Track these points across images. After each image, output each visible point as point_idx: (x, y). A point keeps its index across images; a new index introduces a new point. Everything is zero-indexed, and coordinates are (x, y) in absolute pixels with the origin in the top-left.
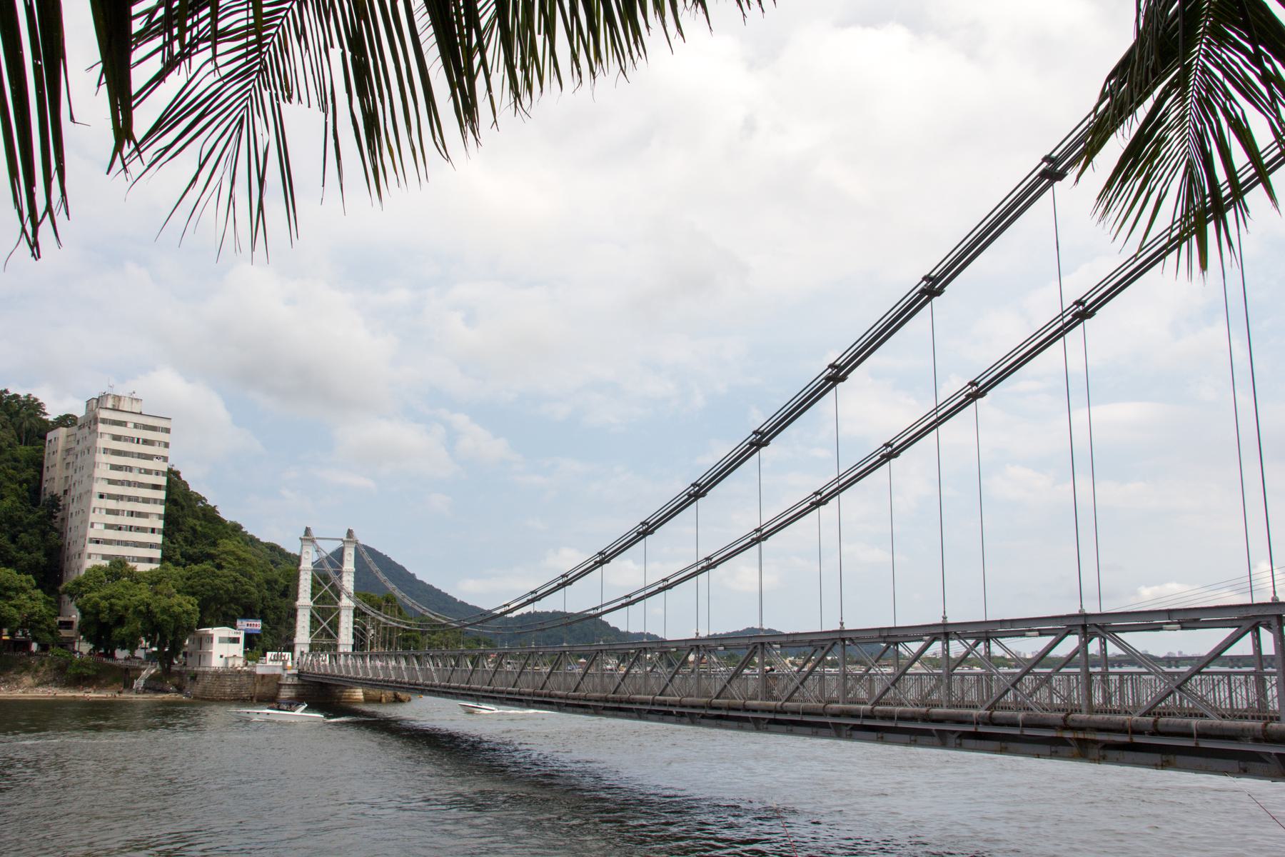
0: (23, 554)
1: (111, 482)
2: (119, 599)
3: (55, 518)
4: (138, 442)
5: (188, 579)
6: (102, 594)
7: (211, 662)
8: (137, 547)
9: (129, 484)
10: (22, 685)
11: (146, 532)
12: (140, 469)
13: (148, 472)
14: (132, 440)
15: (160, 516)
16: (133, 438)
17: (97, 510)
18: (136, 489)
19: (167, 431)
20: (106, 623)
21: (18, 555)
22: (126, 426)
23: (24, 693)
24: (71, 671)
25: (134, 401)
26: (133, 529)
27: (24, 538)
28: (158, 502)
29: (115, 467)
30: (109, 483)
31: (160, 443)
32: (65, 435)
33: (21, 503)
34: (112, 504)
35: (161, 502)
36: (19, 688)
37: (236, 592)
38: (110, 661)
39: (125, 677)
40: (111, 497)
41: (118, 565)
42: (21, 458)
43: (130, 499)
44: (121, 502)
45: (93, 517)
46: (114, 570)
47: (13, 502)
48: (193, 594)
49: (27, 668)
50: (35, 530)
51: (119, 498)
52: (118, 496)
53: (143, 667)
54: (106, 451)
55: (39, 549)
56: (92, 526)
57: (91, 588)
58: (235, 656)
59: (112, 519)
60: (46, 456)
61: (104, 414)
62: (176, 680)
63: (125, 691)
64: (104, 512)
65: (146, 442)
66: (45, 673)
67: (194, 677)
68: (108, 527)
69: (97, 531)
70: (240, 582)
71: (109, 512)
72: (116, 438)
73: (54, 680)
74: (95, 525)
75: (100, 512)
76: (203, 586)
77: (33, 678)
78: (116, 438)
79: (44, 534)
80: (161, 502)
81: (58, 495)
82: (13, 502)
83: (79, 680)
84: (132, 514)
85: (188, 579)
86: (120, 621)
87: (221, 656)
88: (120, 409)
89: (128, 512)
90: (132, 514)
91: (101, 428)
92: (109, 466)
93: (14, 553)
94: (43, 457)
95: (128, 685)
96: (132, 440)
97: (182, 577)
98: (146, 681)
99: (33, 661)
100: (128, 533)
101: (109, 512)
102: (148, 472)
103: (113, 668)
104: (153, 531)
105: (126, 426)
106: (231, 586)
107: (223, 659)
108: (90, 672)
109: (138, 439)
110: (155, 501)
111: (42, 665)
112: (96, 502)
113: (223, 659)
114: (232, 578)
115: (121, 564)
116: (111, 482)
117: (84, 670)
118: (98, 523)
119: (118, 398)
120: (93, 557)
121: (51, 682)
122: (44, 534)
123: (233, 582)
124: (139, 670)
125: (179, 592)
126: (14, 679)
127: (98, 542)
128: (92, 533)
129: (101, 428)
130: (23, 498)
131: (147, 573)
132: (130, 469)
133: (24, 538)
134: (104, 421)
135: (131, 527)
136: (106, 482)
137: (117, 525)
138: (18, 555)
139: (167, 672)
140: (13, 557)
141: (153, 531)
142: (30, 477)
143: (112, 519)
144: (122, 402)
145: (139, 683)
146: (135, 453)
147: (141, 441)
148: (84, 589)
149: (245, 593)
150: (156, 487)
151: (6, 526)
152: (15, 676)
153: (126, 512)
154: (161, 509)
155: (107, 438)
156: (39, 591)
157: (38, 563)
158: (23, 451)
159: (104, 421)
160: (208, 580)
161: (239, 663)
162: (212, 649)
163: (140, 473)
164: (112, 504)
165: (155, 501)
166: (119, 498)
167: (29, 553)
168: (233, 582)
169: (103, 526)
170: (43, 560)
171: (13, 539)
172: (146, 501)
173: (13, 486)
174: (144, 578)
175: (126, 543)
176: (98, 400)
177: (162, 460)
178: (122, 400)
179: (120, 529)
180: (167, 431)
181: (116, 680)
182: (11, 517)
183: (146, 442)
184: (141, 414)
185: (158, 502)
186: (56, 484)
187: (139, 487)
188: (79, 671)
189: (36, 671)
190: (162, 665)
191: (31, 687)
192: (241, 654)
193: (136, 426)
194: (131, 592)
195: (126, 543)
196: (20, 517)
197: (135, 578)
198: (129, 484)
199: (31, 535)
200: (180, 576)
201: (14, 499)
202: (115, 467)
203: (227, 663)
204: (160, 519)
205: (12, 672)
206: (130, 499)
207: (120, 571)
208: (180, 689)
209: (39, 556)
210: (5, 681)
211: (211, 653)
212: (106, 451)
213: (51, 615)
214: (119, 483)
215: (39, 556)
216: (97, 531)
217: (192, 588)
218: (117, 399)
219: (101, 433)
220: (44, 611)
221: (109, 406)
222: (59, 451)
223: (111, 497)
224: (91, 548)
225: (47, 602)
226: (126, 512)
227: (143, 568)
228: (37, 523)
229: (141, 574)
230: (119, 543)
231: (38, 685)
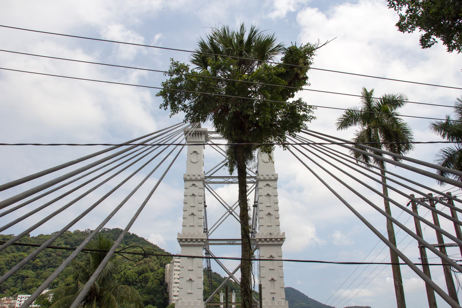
3: (167, 289)
17: (175, 287)
27: (158, 295)
45: (174, 289)
50: (161, 293)
54: (176, 270)
56: (174, 291)
64: (177, 287)
79: (163, 294)
82: (155, 285)
112: (175, 285)
120: (175, 301)
127: (175, 296)
128: (174, 294)
133: (158, 295)
140: (155, 301)
196: (157, 290)
209: (161, 301)
212: (176, 270)
215: (161, 301)
224: (174, 298)
228: (161, 291)
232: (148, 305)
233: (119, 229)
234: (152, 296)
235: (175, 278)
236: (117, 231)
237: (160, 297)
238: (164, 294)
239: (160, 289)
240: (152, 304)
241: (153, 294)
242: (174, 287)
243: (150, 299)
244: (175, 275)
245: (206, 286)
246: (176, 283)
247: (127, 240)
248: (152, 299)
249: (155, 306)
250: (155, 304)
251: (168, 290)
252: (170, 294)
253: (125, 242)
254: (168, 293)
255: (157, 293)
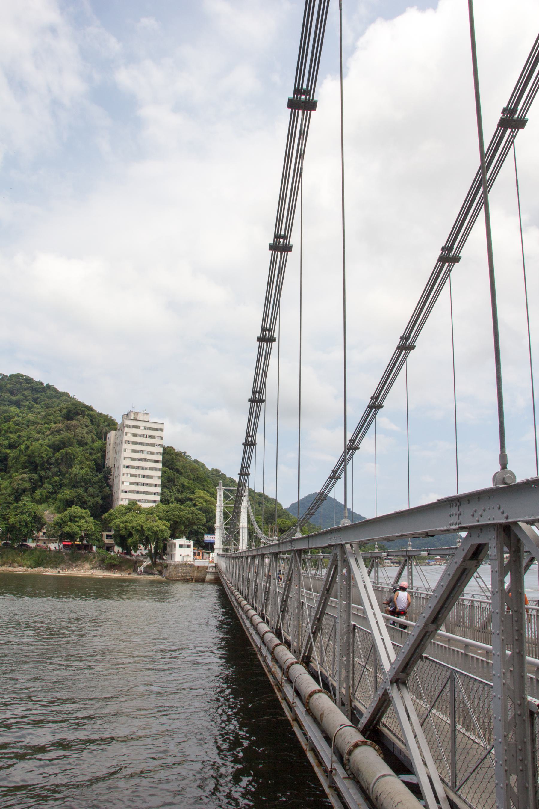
0: (90, 499)
1: (133, 459)
2: (130, 523)
3: (110, 479)
4: (146, 437)
5: (167, 512)
6: (122, 520)
7: (175, 559)
8: (147, 494)
9: (142, 460)
10: (84, 568)
11: (152, 486)
12: (148, 452)
13: (152, 453)
14: (143, 436)
15: (159, 478)
16: (144, 435)
17: (125, 475)
18: (146, 462)
19: (162, 430)
20: (124, 536)
21: (88, 499)
22: (139, 428)
23: (84, 572)
24: (106, 562)
25: (145, 415)
26: (144, 485)
27: (91, 490)
28: (158, 469)
29: (134, 451)
30: (131, 460)
31: (158, 437)
32: (114, 435)
33: (91, 472)
34: (133, 471)
35: (160, 470)
36: (83, 569)
37: (192, 519)
38: (128, 557)
39: (134, 565)
40: (133, 467)
41: (132, 504)
42: (95, 448)
43: (143, 468)
44: (138, 470)
45: (123, 479)
46: (130, 507)
47: (87, 471)
48: (169, 520)
49: (87, 559)
50: (96, 486)
51: (137, 468)
52: (136, 467)
53: (144, 560)
54: (129, 442)
55: (98, 496)
57: (117, 517)
58: (188, 555)
59: (133, 480)
60: (107, 446)
61: (128, 422)
62: (159, 568)
63: (134, 573)
64: (129, 475)
65: (150, 437)
66: (95, 562)
67: (166, 567)
68: (132, 483)
69: (126, 486)
70: (195, 514)
71: (132, 475)
72: (135, 435)
73: (100, 566)
74: (124, 483)
75: (127, 476)
76: (174, 516)
77: (90, 565)
78: (135, 435)
79: (102, 487)
80: (160, 470)
81: (110, 467)
82: (87, 471)
83: (111, 567)
84: (144, 476)
85: (167, 512)
86: (130, 535)
87: (181, 555)
88: (138, 419)
89: (142, 475)
90: (144, 476)
91: (126, 430)
92: (131, 450)
93: (86, 498)
94: (106, 447)
95: (135, 570)
96: (143, 436)
97: (164, 511)
98: (145, 568)
99: (91, 556)
100: (142, 487)
101: (132, 475)
102: (152, 453)
103: (129, 560)
104: (155, 485)
105: (139, 428)
106: (190, 516)
107: (182, 557)
108: (116, 562)
109: (146, 436)
110: (156, 469)
111: (94, 558)
112: (125, 470)
113: (182, 557)
114: (191, 511)
115: (134, 504)
116: (133, 459)
117: (113, 561)
118: (126, 482)
119: (137, 414)
120: (124, 500)
121: (99, 567)
122: (102, 487)
123: (192, 514)
124: (142, 562)
125: (160, 519)
126: (81, 565)
127: (126, 492)
128: (123, 487)
129: (126, 430)
130: (92, 469)
131: (147, 508)
132: (142, 452)
133: (91, 490)
134: (128, 426)
135: (144, 483)
136: (130, 459)
137: (136, 483)
138: (88, 499)
139: (154, 564)
140: (85, 500)
141: (155, 485)
142: (96, 457)
143: (133, 480)
144: (139, 416)
145: (141, 569)
146: (145, 443)
147: (148, 436)
148: (113, 517)
149: (198, 519)
150: (157, 461)
151: (83, 484)
152: (81, 563)
153: (140, 476)
154: (160, 474)
155: (130, 435)
156: (92, 518)
157: (97, 503)
158: (98, 443)
159: (128, 426)
160: (177, 512)
161: (190, 559)
162: (175, 551)
163: (148, 454)
164: (133, 471)
165: (156, 469)
166: (137, 468)
167: (93, 498)
168: (192, 514)
169: (129, 483)
170: (100, 502)
171: (86, 490)
172: (151, 469)
173: (88, 463)
174: (145, 511)
175: (142, 493)
176: (127, 415)
177: (159, 446)
178: (139, 414)
179: (138, 485)
180: (162, 430)
181: (130, 567)
182: (85, 479)
183: (150, 437)
184: (149, 421)
185: (158, 469)
186: (110, 461)
187: (147, 462)
188: (110, 562)
189: (91, 561)
190: (152, 560)
191: (89, 569)
192: (192, 554)
193: (145, 428)
194: (136, 519)
195: (142, 493)
197: (140, 511)
198: (142, 460)
199: (94, 488)
200: (163, 510)
201: (87, 469)
202: (134, 451)
203: (183, 559)
204: (159, 479)
205: (80, 561)
206: (143, 468)
207: (133, 507)
208: (161, 573)
209: (98, 500)
210: (76, 566)
211: (175, 553)
212: (129, 442)
213: (98, 531)
214: (137, 460)
215: (98, 500)
216: (126, 486)
217: (168, 517)
218: (136, 414)
219: (126, 433)
220: (93, 529)
221: (132, 418)
222: (112, 444)
223: (133, 467)
224: (123, 495)
225: (96, 524)
226: (140, 476)
227: (144, 505)
228: (98, 482)
229: (144, 510)
230: (137, 492)
231: (92, 568)
232: (71, 507)
233: (22, 375)
234: (80, 491)
235: (125, 458)
236: (19, 379)
237: (96, 493)
238: (104, 487)
239: (96, 479)
240: (80, 506)
241: (82, 487)
242: (123, 475)
243: (76, 497)
244: (125, 451)
245: (185, 477)
246: (128, 467)
247: (36, 396)
248: (79, 496)
249: (85, 509)
250: (85, 506)
251: (111, 480)
252: (115, 489)
253: (32, 398)
254: (111, 487)
255: (89, 485)
